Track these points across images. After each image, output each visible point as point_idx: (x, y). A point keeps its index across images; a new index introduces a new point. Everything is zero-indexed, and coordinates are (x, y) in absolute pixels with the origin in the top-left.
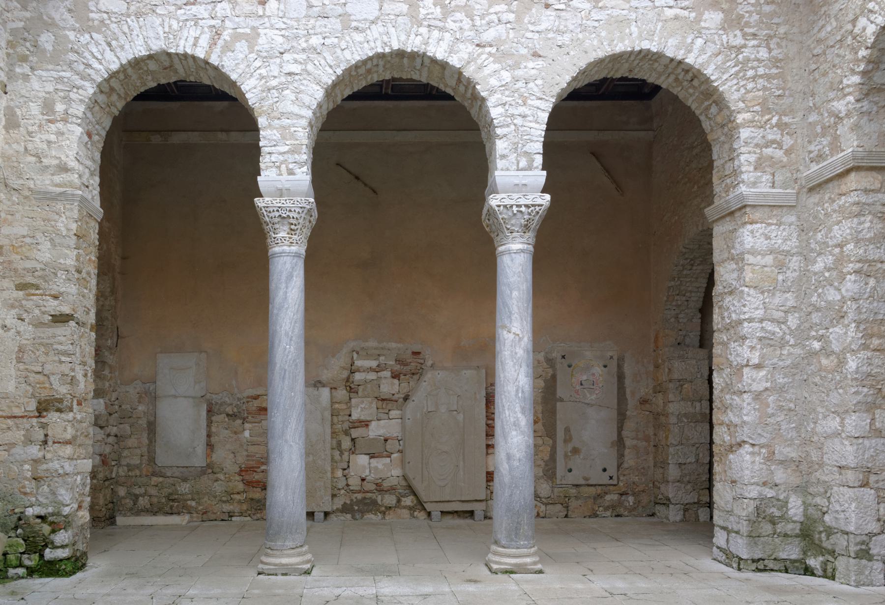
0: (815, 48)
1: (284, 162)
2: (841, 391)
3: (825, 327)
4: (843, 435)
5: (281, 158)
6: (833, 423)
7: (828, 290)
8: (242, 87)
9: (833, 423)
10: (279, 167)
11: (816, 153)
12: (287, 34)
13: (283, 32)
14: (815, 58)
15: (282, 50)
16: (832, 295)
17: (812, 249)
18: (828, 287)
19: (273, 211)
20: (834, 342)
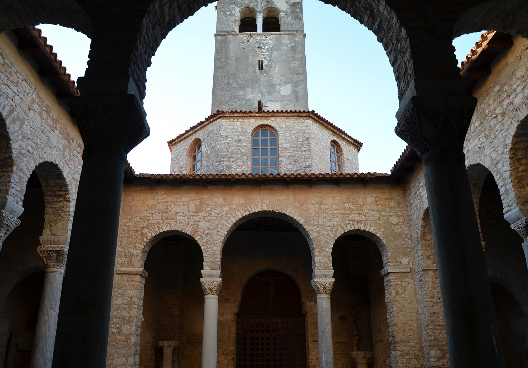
0: (123, 227)
1: (17, 195)
2: (127, 348)
3: (120, 324)
4: (127, 365)
5: (16, 193)
6: (122, 360)
7: (123, 312)
8: (12, 144)
9: (122, 360)
10: (14, 197)
11: (121, 262)
12: (32, 131)
13: (31, 129)
14: (123, 230)
15: (29, 138)
16: (125, 313)
17: (116, 295)
18: (123, 310)
19: (6, 221)
20: (124, 330)
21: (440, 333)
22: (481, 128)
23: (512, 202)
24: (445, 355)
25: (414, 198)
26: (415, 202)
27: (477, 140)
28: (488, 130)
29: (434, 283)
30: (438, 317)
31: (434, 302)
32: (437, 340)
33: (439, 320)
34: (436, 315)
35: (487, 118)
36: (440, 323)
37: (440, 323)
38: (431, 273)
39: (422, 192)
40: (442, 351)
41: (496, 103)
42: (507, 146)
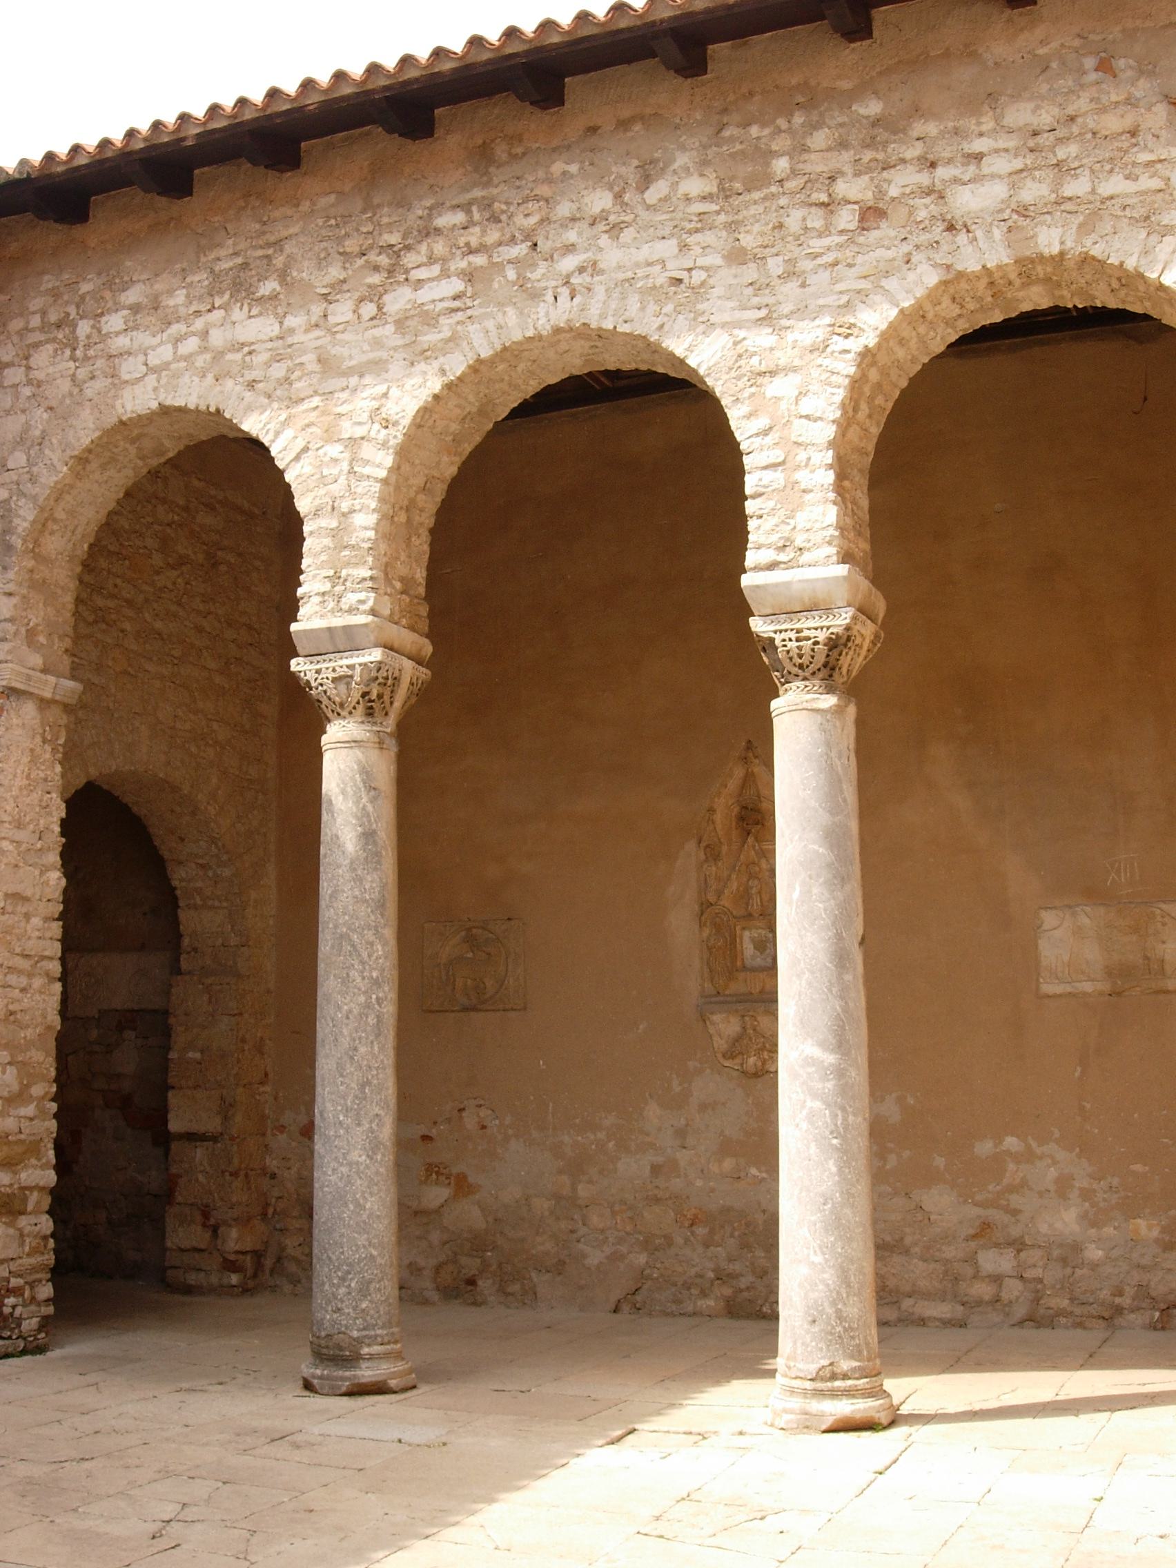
21: (23, 990)
22: (718, 213)
23: (817, 537)
24: (28, 1086)
25: (36, 345)
26: (32, 362)
27: (670, 246)
28: (762, 234)
29: (34, 760)
30: (27, 916)
31: (24, 847)
32: (12, 1018)
33: (29, 927)
34: (22, 909)
35: (773, 189)
36: (31, 942)
37: (32, 946)
38: (29, 710)
39: (118, 334)
40: (22, 1066)
41: (847, 156)
42: (855, 331)
